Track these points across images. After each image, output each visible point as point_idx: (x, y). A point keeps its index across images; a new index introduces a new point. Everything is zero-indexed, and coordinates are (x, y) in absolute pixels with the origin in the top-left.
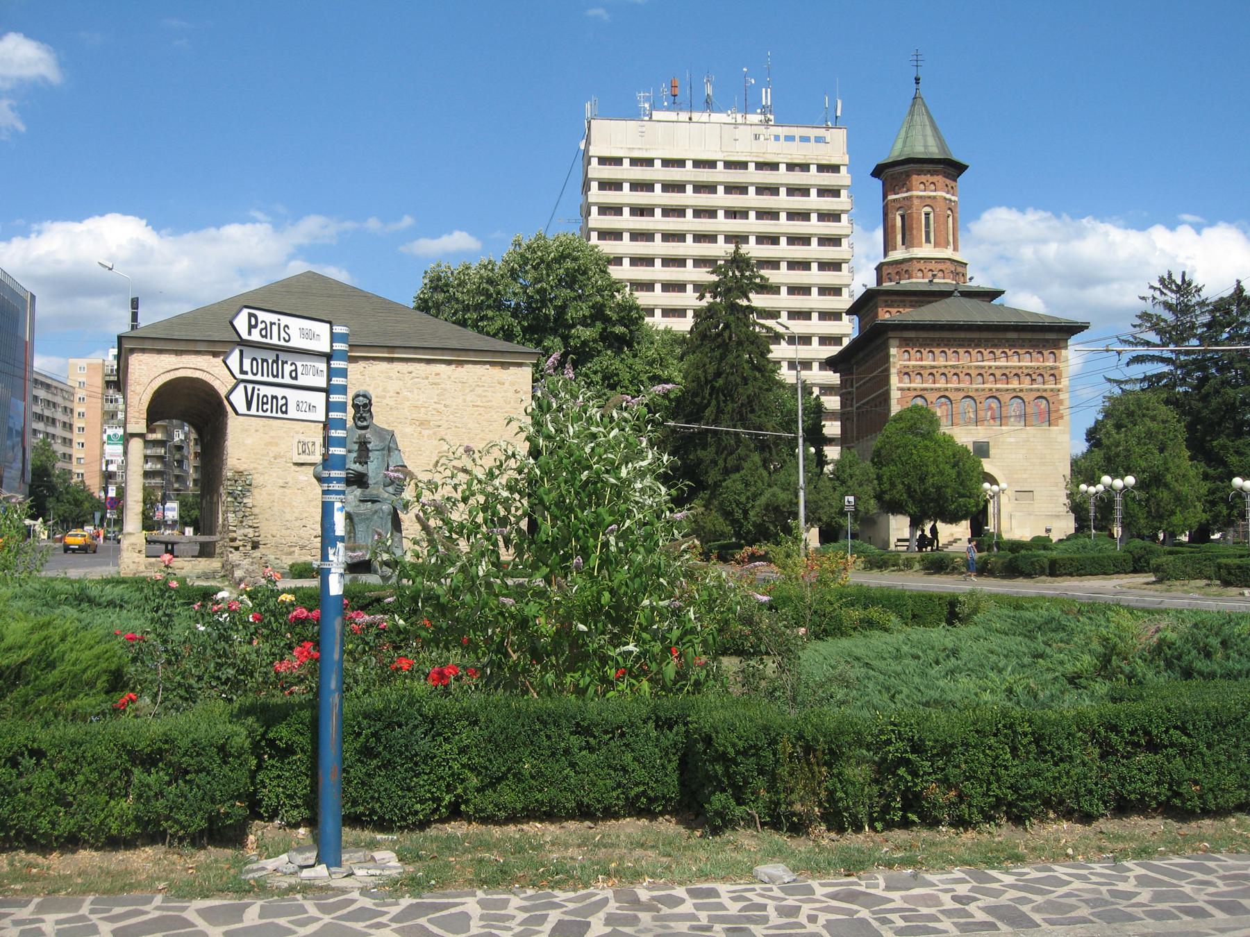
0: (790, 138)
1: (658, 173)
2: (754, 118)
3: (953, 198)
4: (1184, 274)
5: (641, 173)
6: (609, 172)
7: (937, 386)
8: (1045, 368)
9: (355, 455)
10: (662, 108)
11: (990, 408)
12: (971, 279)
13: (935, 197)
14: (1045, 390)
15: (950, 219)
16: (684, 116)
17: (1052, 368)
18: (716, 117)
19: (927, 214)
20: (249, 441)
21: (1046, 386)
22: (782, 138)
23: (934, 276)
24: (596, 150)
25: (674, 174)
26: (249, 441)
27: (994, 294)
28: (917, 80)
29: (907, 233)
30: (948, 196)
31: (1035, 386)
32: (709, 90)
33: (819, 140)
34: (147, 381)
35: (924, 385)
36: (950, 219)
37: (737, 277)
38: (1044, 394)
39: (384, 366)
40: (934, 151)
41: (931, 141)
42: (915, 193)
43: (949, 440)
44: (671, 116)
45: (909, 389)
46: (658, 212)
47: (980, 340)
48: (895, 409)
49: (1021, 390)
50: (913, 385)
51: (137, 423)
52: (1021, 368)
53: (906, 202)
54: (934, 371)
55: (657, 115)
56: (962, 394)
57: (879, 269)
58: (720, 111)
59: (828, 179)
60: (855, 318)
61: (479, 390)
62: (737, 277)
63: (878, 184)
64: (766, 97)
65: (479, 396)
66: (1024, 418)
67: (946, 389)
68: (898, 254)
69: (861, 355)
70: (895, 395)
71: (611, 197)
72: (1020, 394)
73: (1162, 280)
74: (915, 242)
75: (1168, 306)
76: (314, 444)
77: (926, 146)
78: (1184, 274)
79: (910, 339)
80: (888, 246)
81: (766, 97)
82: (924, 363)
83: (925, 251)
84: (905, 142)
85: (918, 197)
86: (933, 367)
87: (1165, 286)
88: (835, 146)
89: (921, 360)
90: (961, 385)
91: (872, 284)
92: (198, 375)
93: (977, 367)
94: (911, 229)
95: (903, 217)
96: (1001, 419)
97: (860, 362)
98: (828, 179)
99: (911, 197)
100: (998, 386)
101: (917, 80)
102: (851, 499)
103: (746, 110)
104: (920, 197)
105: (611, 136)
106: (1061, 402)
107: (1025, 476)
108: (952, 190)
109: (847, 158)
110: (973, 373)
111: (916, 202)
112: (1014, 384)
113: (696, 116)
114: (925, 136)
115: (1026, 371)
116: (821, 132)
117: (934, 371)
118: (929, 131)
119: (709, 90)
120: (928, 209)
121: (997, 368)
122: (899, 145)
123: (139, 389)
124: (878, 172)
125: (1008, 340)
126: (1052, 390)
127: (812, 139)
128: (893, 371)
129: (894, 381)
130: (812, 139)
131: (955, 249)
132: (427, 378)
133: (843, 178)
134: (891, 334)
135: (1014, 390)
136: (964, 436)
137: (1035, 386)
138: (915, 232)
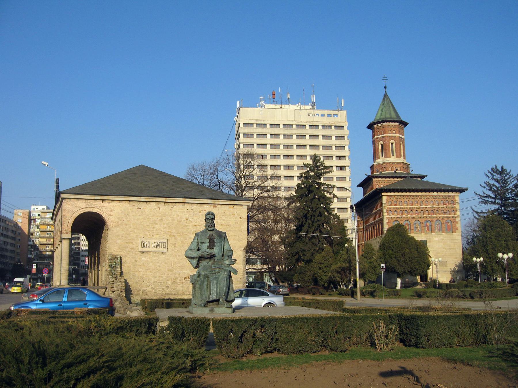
0: (322, 115)
1: (268, 130)
2: (308, 107)
3: (403, 137)
4: (502, 167)
5: (261, 130)
6: (247, 130)
8: (450, 208)
9: (208, 244)
11: (427, 226)
12: (412, 171)
13: (395, 136)
14: (450, 217)
15: (402, 146)
16: (278, 106)
18: (292, 107)
19: (392, 144)
20: (119, 242)
22: (320, 115)
23: (397, 170)
24: (242, 121)
25: (275, 131)
26: (119, 242)
27: (423, 177)
28: (385, 88)
30: (401, 136)
31: (446, 216)
32: (288, 96)
33: (336, 116)
34: (71, 213)
35: (399, 216)
36: (402, 146)
37: (316, 169)
39: (181, 206)
40: (394, 117)
41: (393, 113)
43: (413, 238)
44: (273, 106)
45: (392, 218)
46: (268, 146)
48: (386, 227)
49: (440, 217)
50: (393, 216)
51: (67, 233)
52: (439, 208)
53: (383, 139)
55: (267, 106)
57: (372, 167)
58: (292, 104)
59: (339, 132)
60: (361, 189)
61: (224, 218)
62: (316, 169)
63: (370, 131)
64: (313, 98)
65: (224, 220)
66: (441, 230)
67: (408, 218)
68: (380, 160)
69: (367, 204)
70: (386, 220)
71: (249, 140)
72: (439, 219)
73: (492, 169)
74: (388, 155)
75: (497, 181)
76: (149, 243)
77: (390, 115)
78: (502, 167)
80: (375, 158)
81: (313, 98)
82: (398, 206)
83: (392, 159)
84: (381, 114)
85: (388, 136)
86: (402, 208)
87: (496, 173)
88: (342, 118)
89: (396, 205)
90: (414, 216)
91: (369, 174)
92: (95, 210)
94: (386, 150)
96: (431, 230)
97: (368, 206)
98: (339, 132)
100: (430, 216)
101: (385, 88)
102: (384, 265)
103: (304, 104)
104: (389, 136)
105: (248, 114)
106: (457, 222)
108: (402, 133)
109: (347, 123)
110: (419, 210)
111: (387, 138)
113: (283, 106)
115: (441, 209)
116: (336, 112)
118: (392, 109)
119: (288, 96)
120: (392, 141)
121: (429, 208)
122: (379, 114)
123: (68, 217)
124: (371, 126)
126: (453, 217)
127: (332, 115)
128: (385, 211)
129: (385, 214)
130: (332, 115)
131: (404, 158)
132: (200, 212)
133: (345, 132)
134: (383, 194)
136: (419, 237)
137: (446, 216)
138: (387, 151)
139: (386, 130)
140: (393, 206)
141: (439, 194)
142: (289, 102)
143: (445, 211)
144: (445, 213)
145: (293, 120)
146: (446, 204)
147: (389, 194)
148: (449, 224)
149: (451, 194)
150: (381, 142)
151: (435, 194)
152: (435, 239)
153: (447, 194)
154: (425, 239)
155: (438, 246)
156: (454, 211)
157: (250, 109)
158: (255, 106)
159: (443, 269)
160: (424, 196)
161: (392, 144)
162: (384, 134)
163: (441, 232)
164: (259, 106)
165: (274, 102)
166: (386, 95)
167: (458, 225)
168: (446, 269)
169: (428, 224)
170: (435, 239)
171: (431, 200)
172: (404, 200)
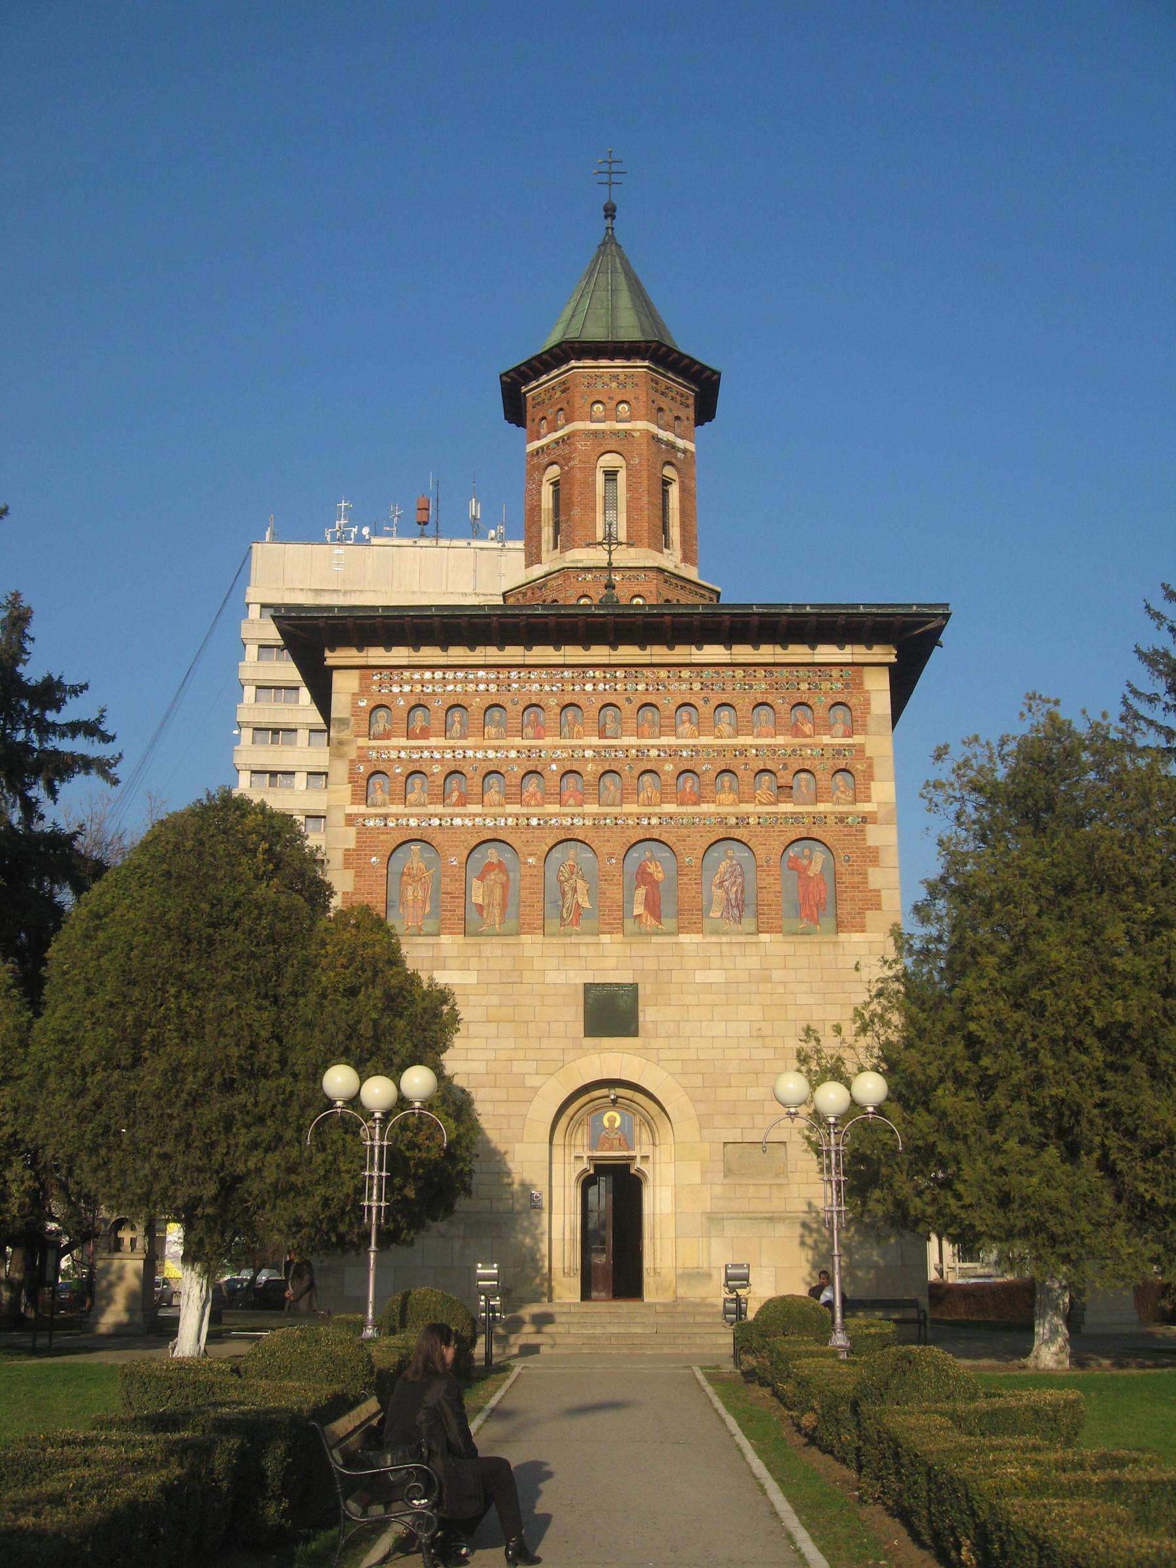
3: (681, 443)
10: (389, 534)
11: (643, 877)
13: (628, 433)
17: (838, 752)
19: (611, 475)
21: (822, 807)
28: (610, 212)
29: (563, 518)
30: (664, 435)
36: (674, 491)
38: (816, 832)
40: (629, 329)
42: (578, 425)
49: (742, 820)
50: (394, 809)
52: (743, 751)
53: (564, 450)
55: (374, 541)
66: (748, 909)
89: (425, 734)
95: (555, 484)
99: (570, 436)
101: (610, 212)
104: (595, 433)
106: (872, 856)
107: (754, 1093)
111: (580, 445)
112: (722, 806)
113: (444, 542)
114: (613, 310)
118: (625, 299)
119: (475, 508)
126: (841, 819)
131: (685, 559)
135: (723, 821)
138: (576, 512)
139: (578, 402)
140: (403, 742)
141: (744, 653)
142: (476, 531)
143: (785, 778)
144: (785, 791)
145: (470, 590)
146: (796, 731)
147: (376, 655)
148: (814, 869)
149: (827, 653)
150: (554, 471)
151: (714, 653)
152: (700, 976)
153: (798, 653)
154: (624, 977)
155: (719, 1029)
156: (850, 771)
157: (290, 548)
158: (315, 538)
159: (757, 1206)
161: (611, 475)
162: (568, 421)
163: (749, 923)
164: (333, 534)
165: (422, 535)
166: (610, 240)
167: (877, 878)
168: (776, 1205)
169: (656, 871)
170: (700, 976)
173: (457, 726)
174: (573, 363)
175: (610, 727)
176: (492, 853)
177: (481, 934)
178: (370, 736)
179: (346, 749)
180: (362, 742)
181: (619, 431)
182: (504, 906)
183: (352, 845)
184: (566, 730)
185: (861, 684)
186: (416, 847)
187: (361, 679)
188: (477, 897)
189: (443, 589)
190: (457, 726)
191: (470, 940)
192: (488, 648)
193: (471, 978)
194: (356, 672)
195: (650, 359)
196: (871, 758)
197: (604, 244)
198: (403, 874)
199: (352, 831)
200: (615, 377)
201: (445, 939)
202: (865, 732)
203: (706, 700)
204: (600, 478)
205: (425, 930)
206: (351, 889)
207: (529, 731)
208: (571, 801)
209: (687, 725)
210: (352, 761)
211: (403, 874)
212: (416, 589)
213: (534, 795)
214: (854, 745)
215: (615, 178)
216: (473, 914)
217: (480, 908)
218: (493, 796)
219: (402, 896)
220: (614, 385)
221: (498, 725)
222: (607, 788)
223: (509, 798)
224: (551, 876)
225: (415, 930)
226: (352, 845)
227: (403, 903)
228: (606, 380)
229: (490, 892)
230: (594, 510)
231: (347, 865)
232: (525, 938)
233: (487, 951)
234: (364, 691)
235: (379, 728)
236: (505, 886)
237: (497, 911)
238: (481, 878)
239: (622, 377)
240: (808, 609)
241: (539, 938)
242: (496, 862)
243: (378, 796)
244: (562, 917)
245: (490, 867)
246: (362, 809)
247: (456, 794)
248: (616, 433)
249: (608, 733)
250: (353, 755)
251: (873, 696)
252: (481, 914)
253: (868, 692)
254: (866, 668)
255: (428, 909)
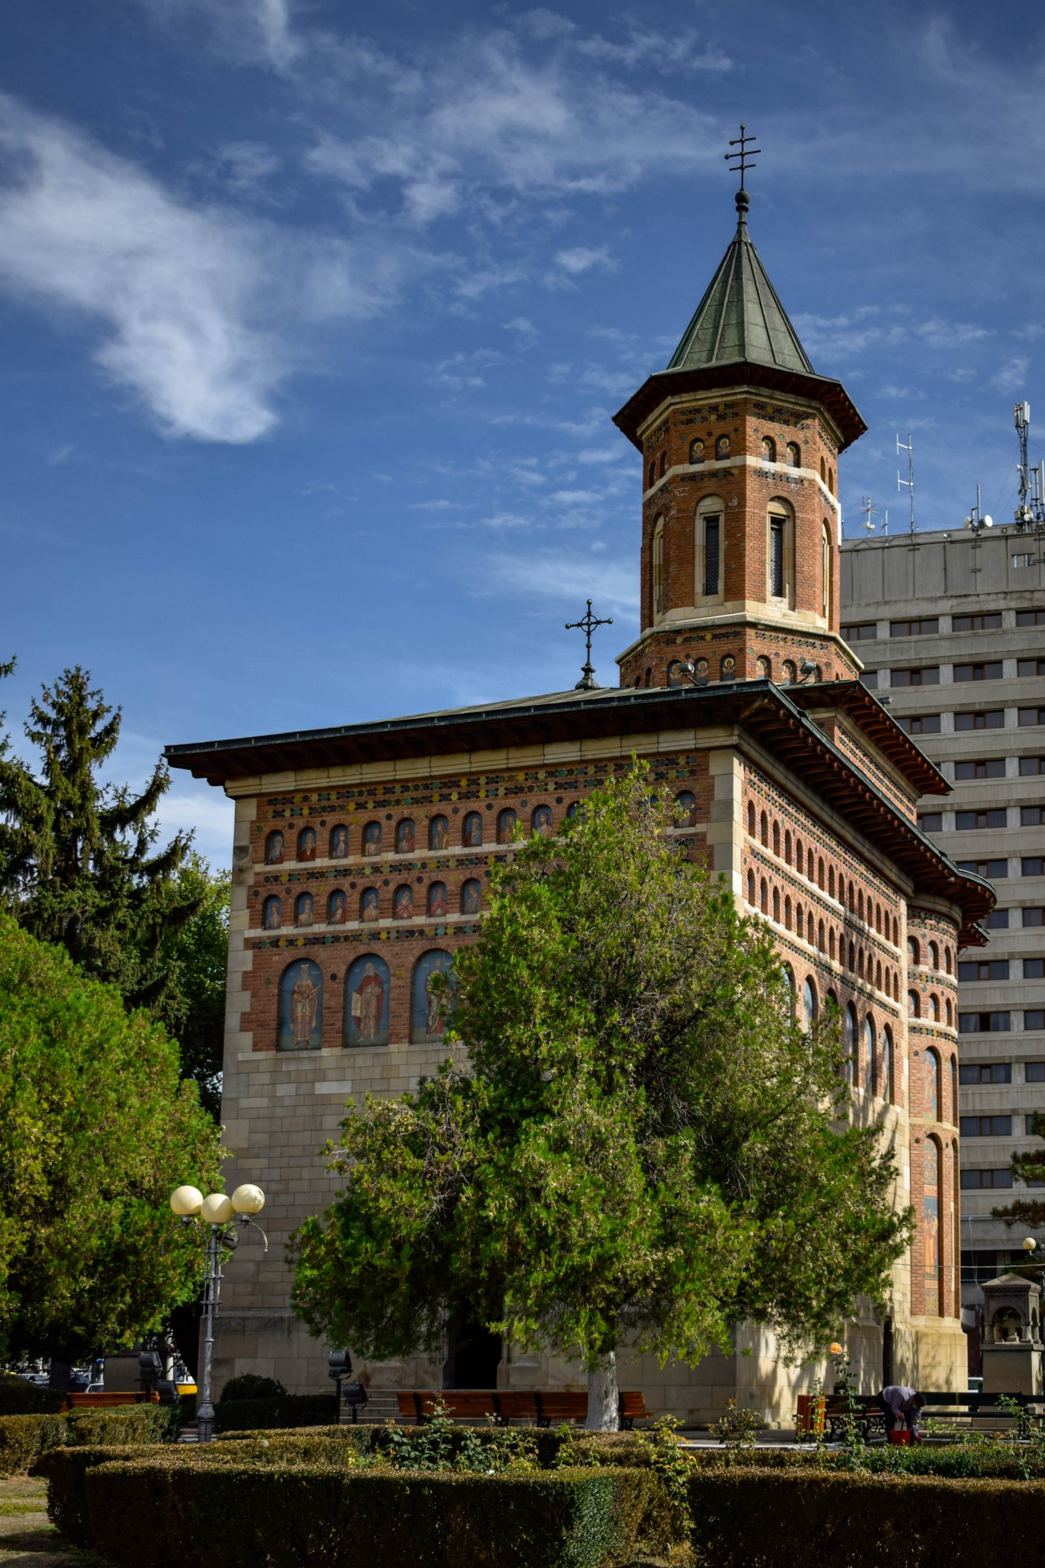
7: (352, 925)
13: (727, 472)
19: (712, 522)
45: (275, 942)
47: (473, 777)
54: (345, 883)
56: (418, 946)
67: (375, 936)
79: (286, 798)
82: (321, 863)
86: (345, 872)
90: (420, 920)
93: (461, 861)
104: (692, 477)
117: (345, 883)
125: (552, 770)
160: (494, 776)
171: (534, 799)
172: (364, 817)
173: (342, 846)
174: (669, 400)
175: (475, 834)
176: (370, 969)
177: (358, 1046)
178: (268, 861)
179: (246, 875)
180: (259, 868)
181: (717, 471)
182: (378, 1017)
183: (249, 967)
184: (436, 840)
185: (707, 769)
186: (305, 966)
187: (258, 807)
188: (356, 1011)
189: (910, 596)
190: (342, 846)
191: (348, 1051)
192: (364, 766)
193: (346, 1088)
194: (254, 801)
195: (749, 384)
196: (712, 847)
197: (734, 243)
198: (294, 992)
199: (250, 953)
200: (714, 408)
201: (325, 1052)
202: (708, 820)
203: (559, 800)
204: (700, 526)
205: (312, 1043)
206: (248, 1010)
207: (404, 844)
208: (439, 911)
209: (545, 826)
210: (250, 887)
211: (294, 992)
212: (880, 598)
213: (406, 907)
214: (696, 834)
215: (748, 160)
216: (353, 1027)
217: (358, 1020)
218: (371, 911)
219: (293, 1012)
220: (713, 417)
221: (378, 840)
222: (471, 896)
223: (382, 915)
224: (420, 984)
225: (303, 1045)
226: (249, 967)
227: (294, 1020)
228: (705, 413)
229: (367, 1004)
230: (692, 563)
231: (245, 987)
232: (393, 1048)
233: (360, 1061)
234: (261, 817)
235: (276, 852)
236: (379, 998)
237: (372, 1023)
238: (360, 991)
239: (721, 408)
240: (632, 700)
241: (405, 1046)
242: (372, 974)
243: (275, 919)
244: (427, 1025)
245: (367, 980)
246: (258, 933)
247: (340, 911)
248: (713, 474)
249: (473, 841)
250: (250, 880)
251: (717, 781)
252: (359, 1026)
253: (713, 777)
254: (712, 753)
255: (314, 1025)
